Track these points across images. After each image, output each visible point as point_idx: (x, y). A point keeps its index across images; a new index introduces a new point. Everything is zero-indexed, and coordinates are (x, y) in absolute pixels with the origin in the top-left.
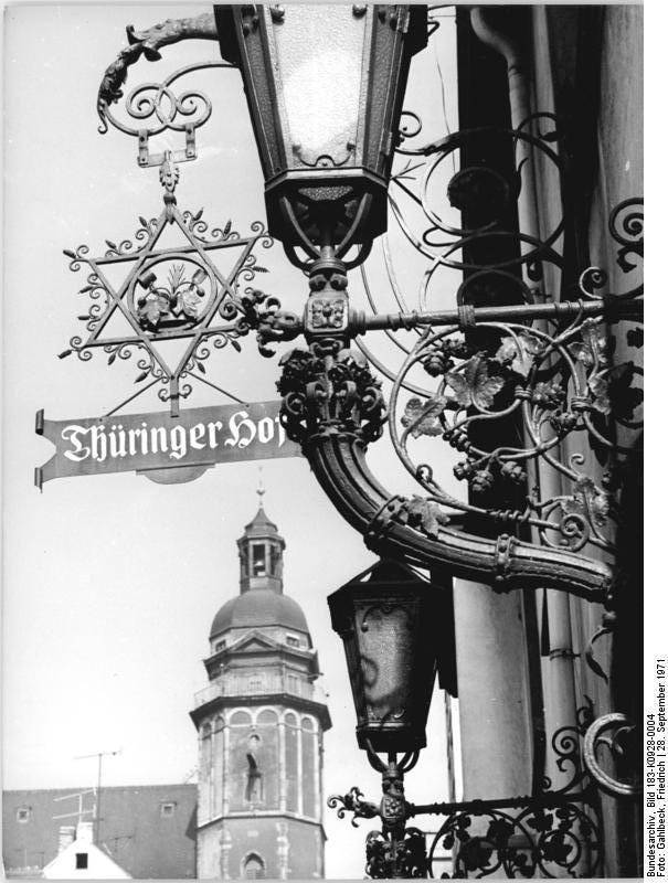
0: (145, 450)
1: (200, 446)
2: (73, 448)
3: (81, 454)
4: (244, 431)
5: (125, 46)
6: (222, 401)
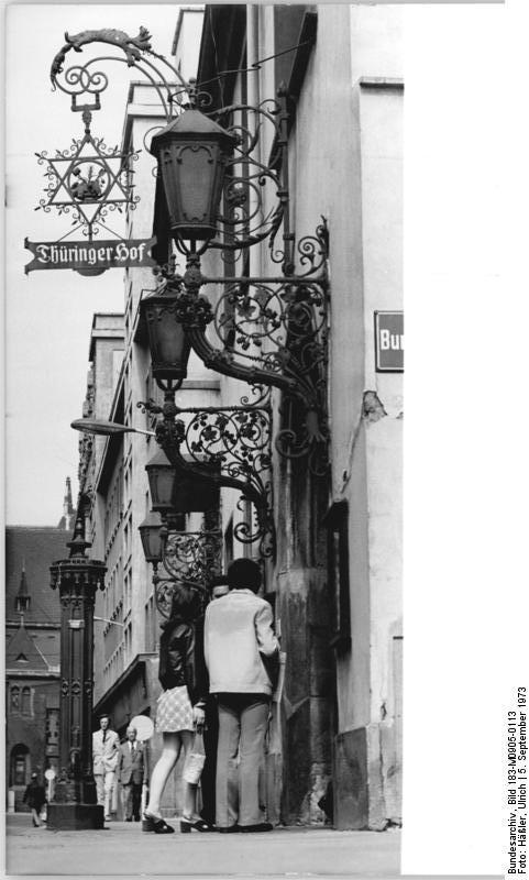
0: (76, 259)
1: (103, 259)
2: (41, 256)
3: (46, 259)
4: (124, 254)
5: (65, 43)
6: (115, 238)
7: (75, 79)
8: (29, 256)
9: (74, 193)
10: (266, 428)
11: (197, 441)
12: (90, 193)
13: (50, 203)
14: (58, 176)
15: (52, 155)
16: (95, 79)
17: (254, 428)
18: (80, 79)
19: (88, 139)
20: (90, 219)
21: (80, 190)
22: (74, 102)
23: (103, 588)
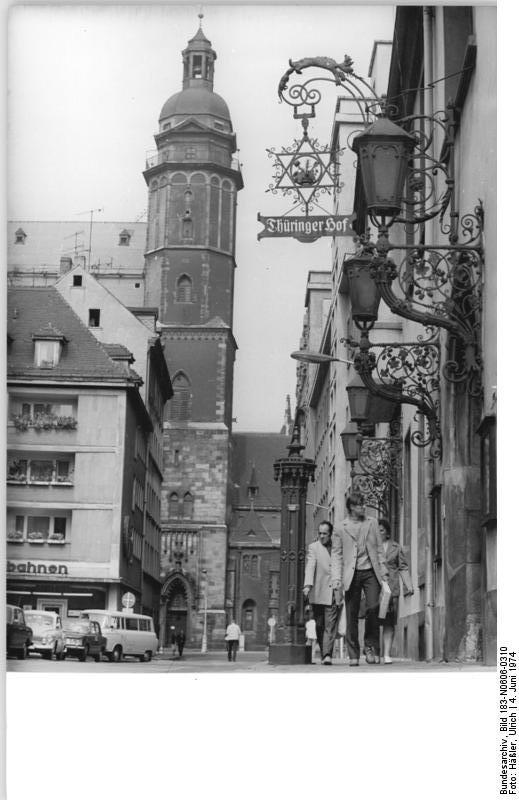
2: (269, 226)
4: (332, 226)
5: (289, 68)
6: (326, 214)
7: (296, 94)
8: (261, 227)
9: (295, 178)
10: (436, 359)
11: (385, 369)
12: (307, 180)
13: (277, 187)
14: (283, 166)
15: (279, 150)
16: (312, 95)
17: (427, 359)
18: (300, 94)
19: (306, 139)
20: (307, 200)
21: (300, 177)
22: (296, 111)
23: (313, 480)
